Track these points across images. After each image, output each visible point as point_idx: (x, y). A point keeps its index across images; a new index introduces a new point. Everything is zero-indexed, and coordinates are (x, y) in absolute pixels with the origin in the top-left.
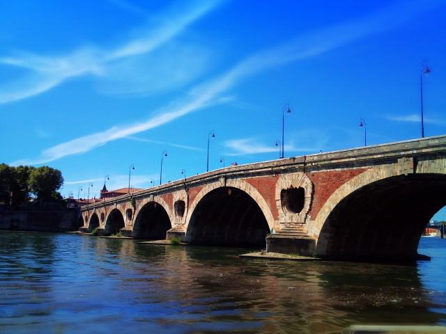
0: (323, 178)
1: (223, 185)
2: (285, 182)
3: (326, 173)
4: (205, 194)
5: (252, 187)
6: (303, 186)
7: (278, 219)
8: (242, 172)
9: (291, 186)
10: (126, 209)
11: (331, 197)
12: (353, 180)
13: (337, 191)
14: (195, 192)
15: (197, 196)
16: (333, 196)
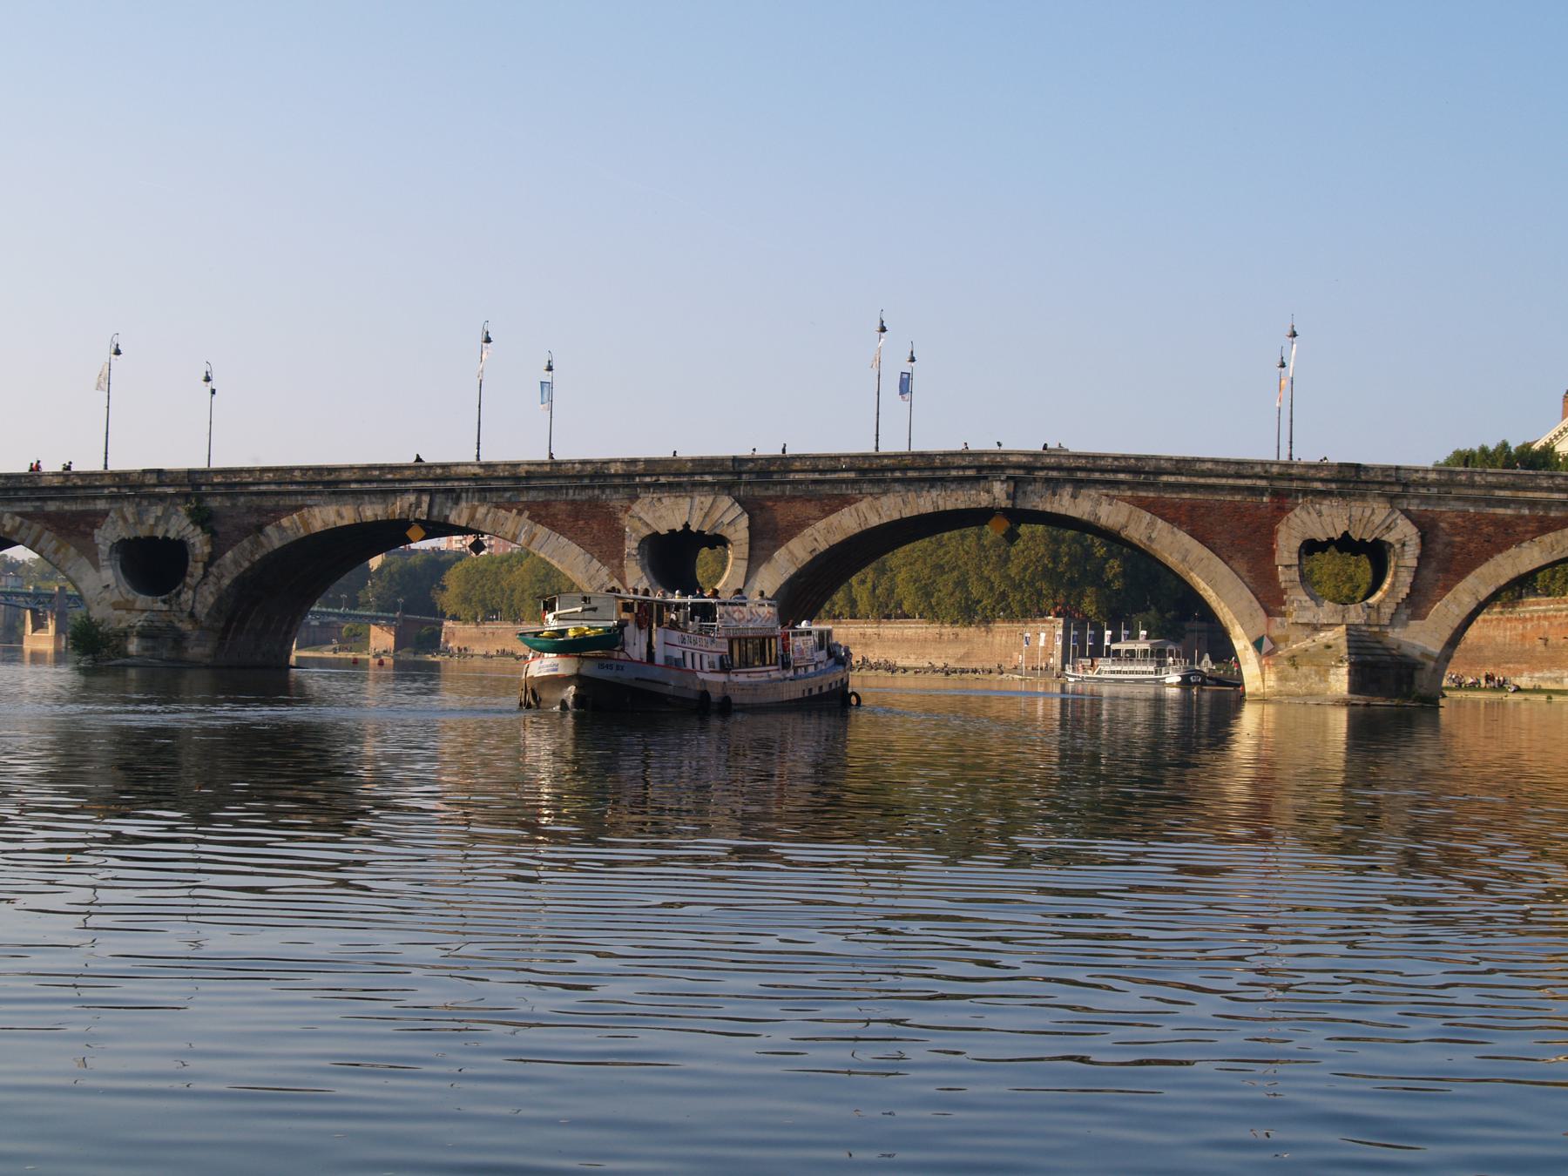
0: (1453, 525)
1: (1005, 503)
2: (1328, 520)
3: (1464, 514)
4: (874, 521)
5: (1160, 523)
6: (1390, 538)
7: (1283, 614)
8: (1121, 476)
9: (1346, 533)
10: (106, 536)
11: (1478, 570)
12: (1549, 538)
13: (1499, 558)
14: (817, 513)
15: (821, 525)
16: (1485, 570)
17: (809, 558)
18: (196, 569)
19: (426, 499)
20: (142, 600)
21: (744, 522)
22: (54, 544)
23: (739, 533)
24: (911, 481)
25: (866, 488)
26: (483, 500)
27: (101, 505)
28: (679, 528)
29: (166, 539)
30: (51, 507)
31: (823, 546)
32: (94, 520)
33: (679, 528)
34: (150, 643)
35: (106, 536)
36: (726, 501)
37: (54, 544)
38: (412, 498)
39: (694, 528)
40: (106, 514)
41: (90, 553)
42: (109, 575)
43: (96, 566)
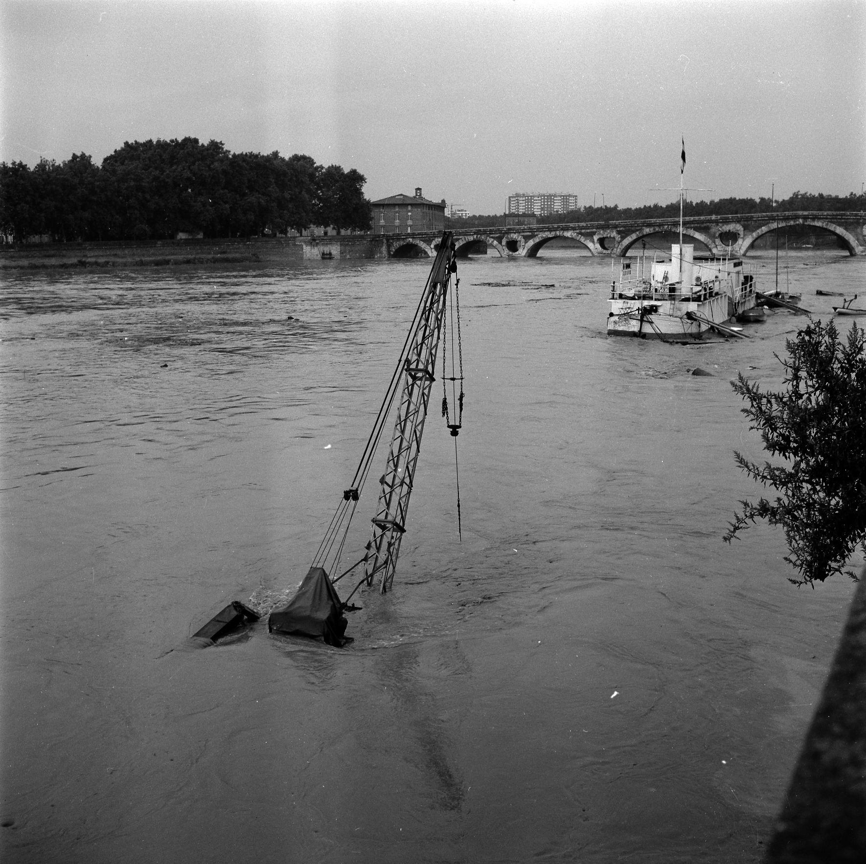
23: (742, 233)
24: (781, 219)
27: (594, 230)
30: (583, 231)
32: (594, 233)
35: (596, 238)
36: (738, 225)
38: (667, 226)
40: (596, 232)
42: (598, 246)
43: (593, 242)
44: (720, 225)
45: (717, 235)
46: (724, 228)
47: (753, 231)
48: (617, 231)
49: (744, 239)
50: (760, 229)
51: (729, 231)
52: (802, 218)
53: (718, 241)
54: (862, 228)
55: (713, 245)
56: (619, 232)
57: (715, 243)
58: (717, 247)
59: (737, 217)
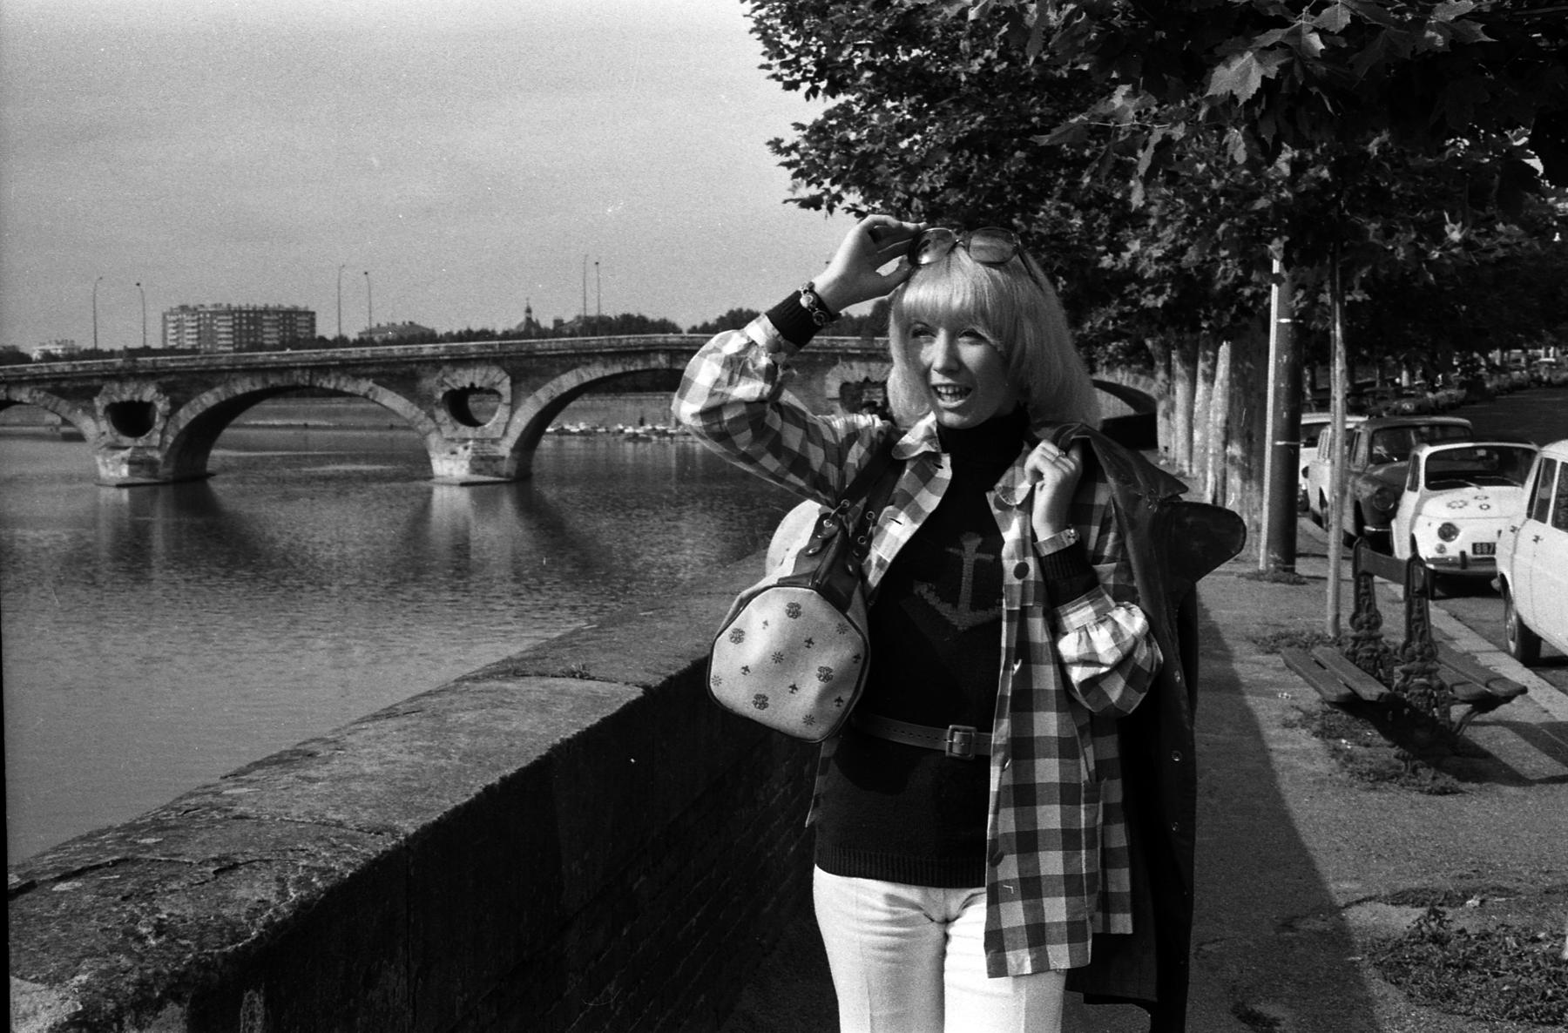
17: (548, 401)
18: (159, 423)
19: (308, 372)
20: (126, 441)
21: (507, 381)
22: (68, 408)
23: (505, 388)
25: (583, 359)
26: (345, 373)
27: (96, 382)
28: (467, 386)
29: (141, 402)
31: (557, 394)
32: (96, 391)
33: (467, 386)
34: (133, 467)
35: (99, 403)
37: (68, 408)
39: (477, 386)
41: (90, 411)
42: (105, 426)
43: (95, 418)
44: (447, 368)
45: (440, 395)
46: (456, 376)
47: (535, 388)
48: (159, 383)
49: (513, 407)
50: (555, 382)
51: (472, 385)
52: (665, 352)
53: (442, 414)
54: (823, 379)
55: (430, 424)
56: (165, 389)
57: (433, 417)
58: (439, 430)
59: (492, 347)
